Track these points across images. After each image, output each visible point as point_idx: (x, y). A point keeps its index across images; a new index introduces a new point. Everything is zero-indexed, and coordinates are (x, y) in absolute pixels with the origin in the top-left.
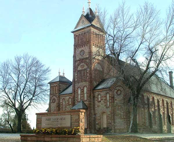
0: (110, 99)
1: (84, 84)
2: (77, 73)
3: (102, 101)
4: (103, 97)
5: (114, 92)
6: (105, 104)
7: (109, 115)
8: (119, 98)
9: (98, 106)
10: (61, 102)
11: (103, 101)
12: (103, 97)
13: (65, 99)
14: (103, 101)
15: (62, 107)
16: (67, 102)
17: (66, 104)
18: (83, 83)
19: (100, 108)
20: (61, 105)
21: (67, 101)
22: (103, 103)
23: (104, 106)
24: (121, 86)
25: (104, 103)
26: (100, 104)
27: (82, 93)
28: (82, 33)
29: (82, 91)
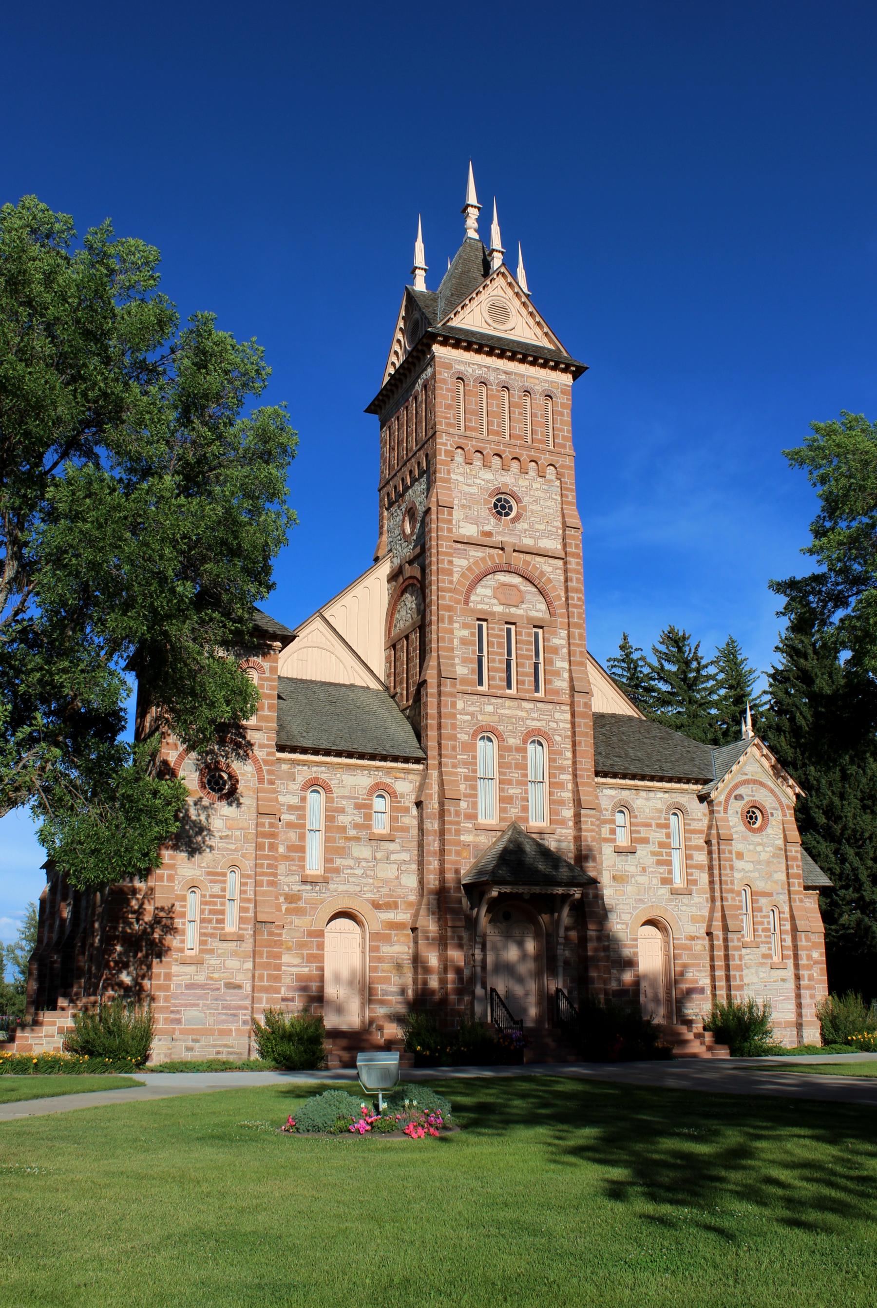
0: (693, 843)
1: (532, 715)
2: (465, 626)
3: (642, 851)
4: (648, 825)
5: (730, 812)
6: (662, 869)
7: (693, 938)
8: (759, 848)
9: (614, 878)
10: (291, 808)
11: (653, 854)
12: (648, 825)
13: (337, 792)
14: (653, 854)
15: (291, 848)
16: (350, 809)
17: (343, 829)
18: (519, 707)
19: (629, 889)
20: (290, 825)
21: (358, 807)
22: (650, 860)
23: (656, 882)
24: (762, 784)
25: (659, 863)
26: (632, 869)
27: (515, 775)
28: (503, 377)
29: (512, 764)
